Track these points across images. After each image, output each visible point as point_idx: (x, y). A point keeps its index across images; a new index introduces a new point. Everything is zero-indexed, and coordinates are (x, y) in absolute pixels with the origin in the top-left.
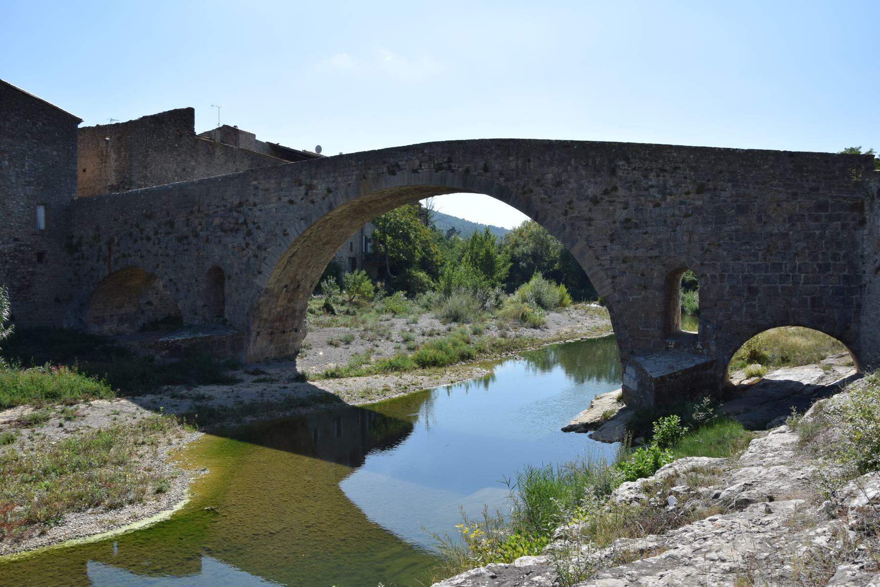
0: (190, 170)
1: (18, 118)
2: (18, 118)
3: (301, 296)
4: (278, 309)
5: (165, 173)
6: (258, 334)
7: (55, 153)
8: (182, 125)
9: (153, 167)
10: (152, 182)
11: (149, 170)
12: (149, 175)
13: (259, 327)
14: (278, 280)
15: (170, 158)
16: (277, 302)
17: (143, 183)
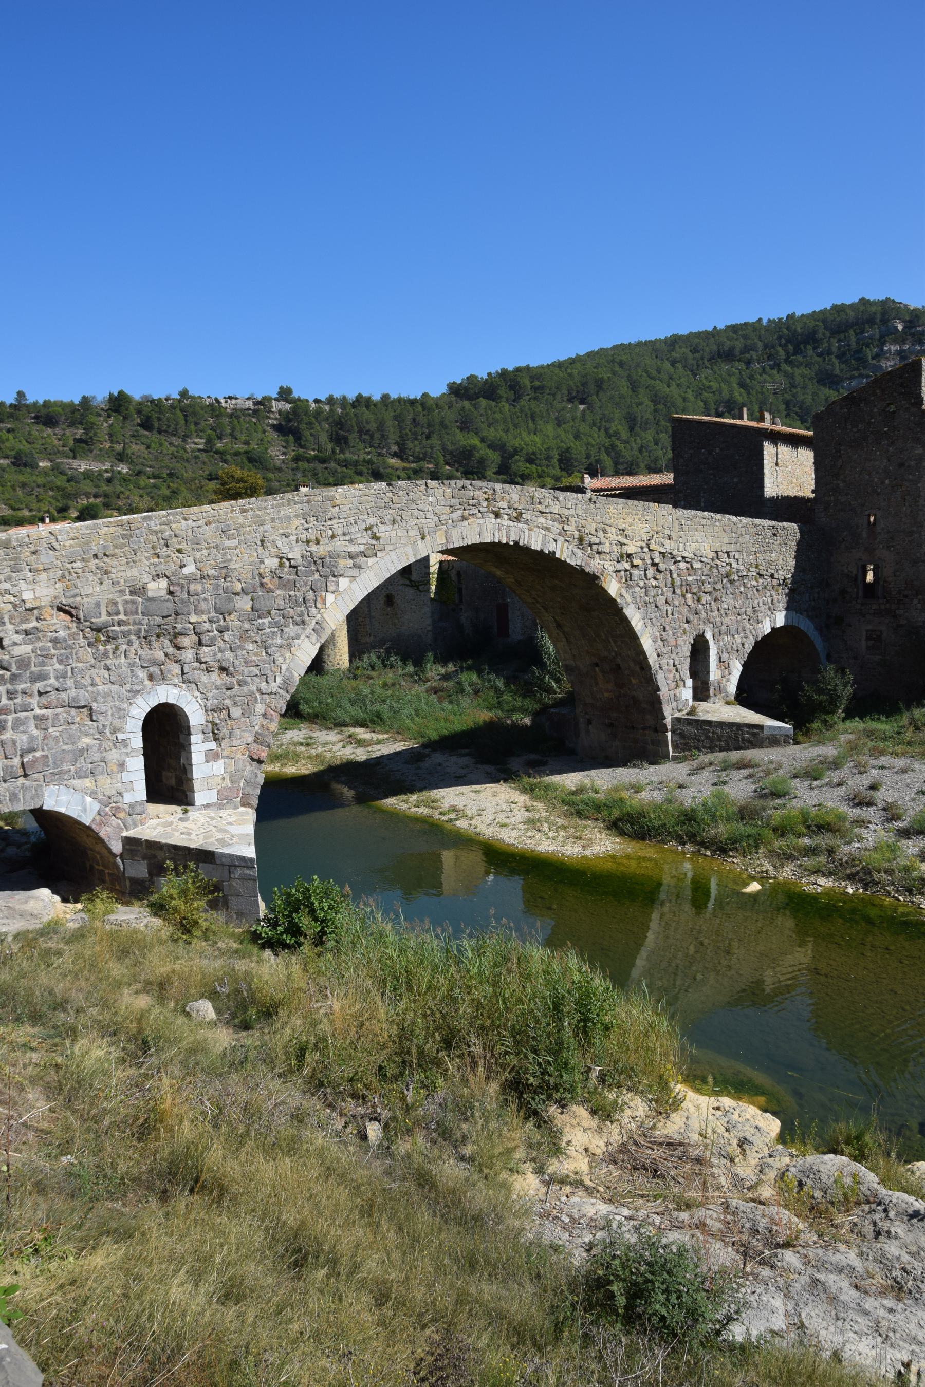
0: (912, 463)
1: (692, 451)
2: (692, 451)
3: (634, 681)
4: (606, 695)
5: (867, 477)
6: (589, 722)
7: (735, 480)
8: (895, 394)
9: (847, 472)
10: (847, 495)
11: (842, 477)
12: (841, 485)
13: (586, 713)
14: (574, 656)
15: (876, 451)
16: (597, 684)
17: (832, 498)
